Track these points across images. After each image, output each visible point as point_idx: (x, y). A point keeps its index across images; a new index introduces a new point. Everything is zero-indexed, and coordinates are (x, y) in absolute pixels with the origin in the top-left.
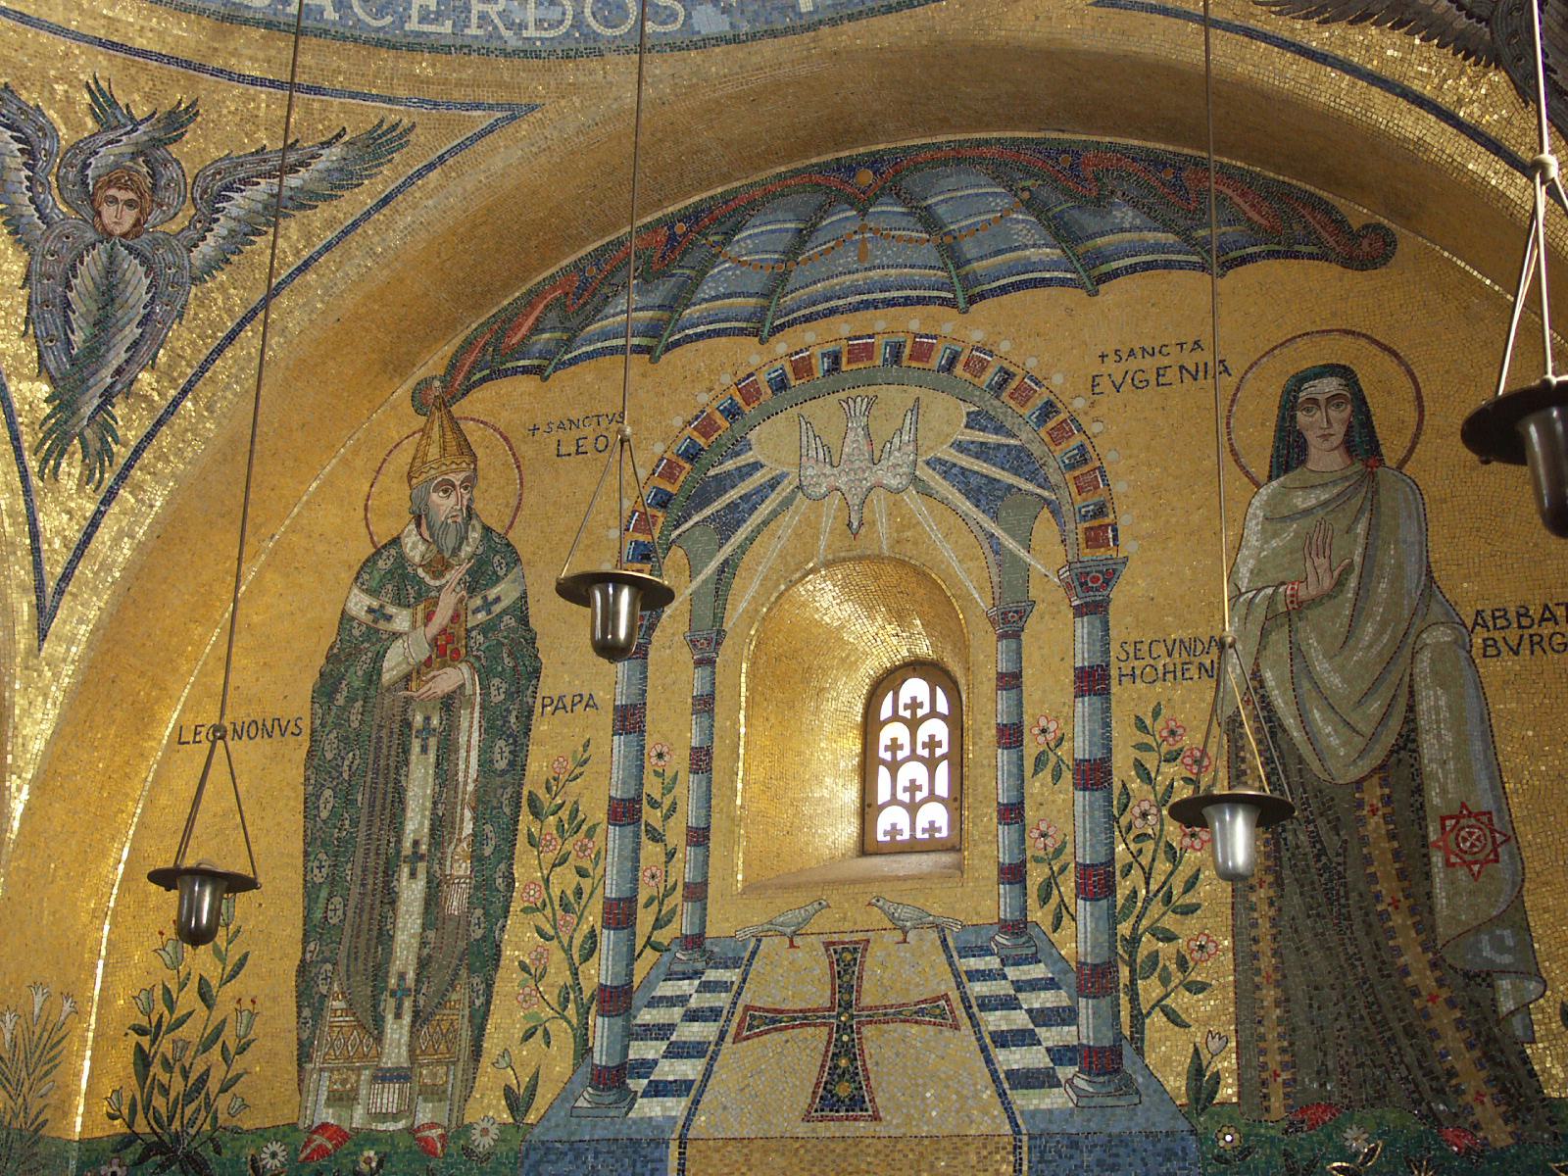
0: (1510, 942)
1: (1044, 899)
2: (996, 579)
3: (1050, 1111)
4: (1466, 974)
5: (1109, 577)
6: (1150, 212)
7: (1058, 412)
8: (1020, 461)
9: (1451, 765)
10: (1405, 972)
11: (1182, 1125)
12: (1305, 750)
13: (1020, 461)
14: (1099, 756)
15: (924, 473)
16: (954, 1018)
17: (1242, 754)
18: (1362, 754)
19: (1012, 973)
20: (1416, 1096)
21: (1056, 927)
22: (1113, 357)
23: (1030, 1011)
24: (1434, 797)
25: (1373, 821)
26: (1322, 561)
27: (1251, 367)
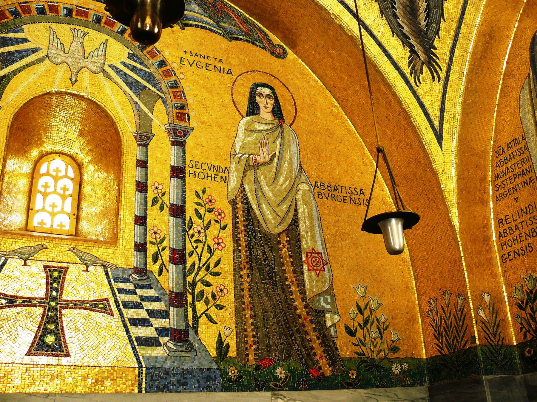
0: (329, 301)
1: (155, 260)
2: (138, 121)
3: (156, 357)
4: (316, 311)
5: (186, 133)
6: (204, 10)
7: (166, 65)
8: (149, 77)
9: (309, 234)
10: (296, 308)
11: (214, 366)
12: (260, 218)
13: (149, 77)
14: (180, 204)
15: (107, 68)
16: (111, 310)
17: (237, 215)
18: (280, 224)
19: (139, 292)
20: (301, 356)
21: (160, 274)
22: (189, 53)
23: (147, 310)
24: (304, 245)
25: (284, 249)
26: (264, 150)
27: (240, 75)
